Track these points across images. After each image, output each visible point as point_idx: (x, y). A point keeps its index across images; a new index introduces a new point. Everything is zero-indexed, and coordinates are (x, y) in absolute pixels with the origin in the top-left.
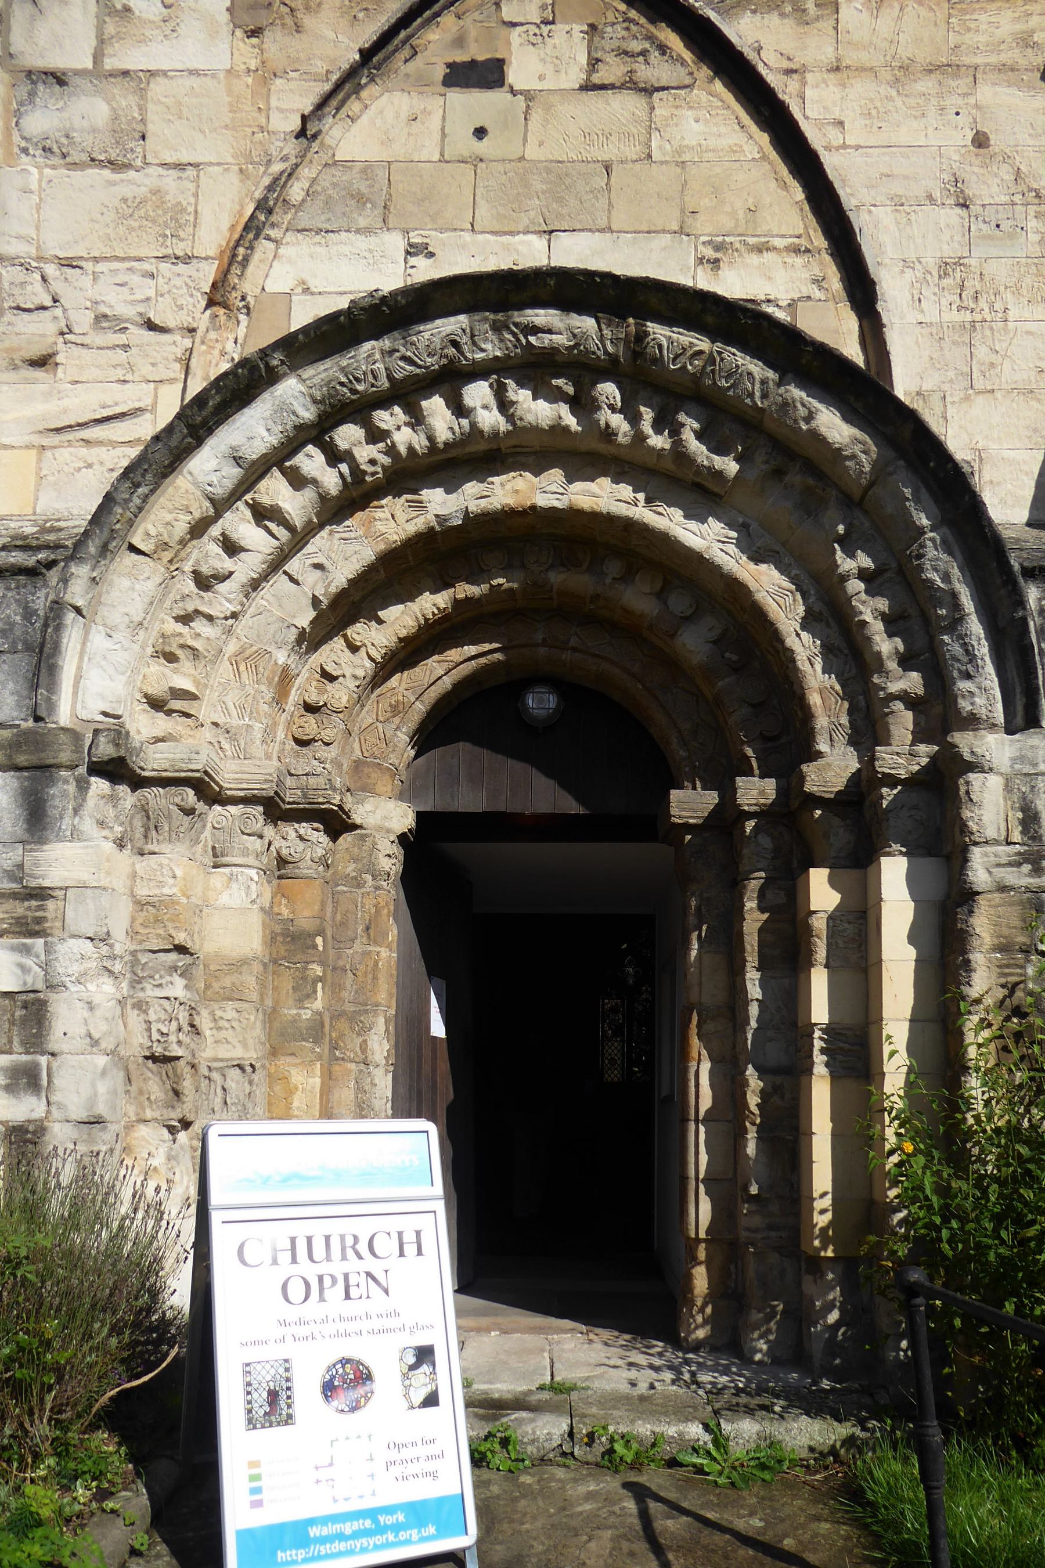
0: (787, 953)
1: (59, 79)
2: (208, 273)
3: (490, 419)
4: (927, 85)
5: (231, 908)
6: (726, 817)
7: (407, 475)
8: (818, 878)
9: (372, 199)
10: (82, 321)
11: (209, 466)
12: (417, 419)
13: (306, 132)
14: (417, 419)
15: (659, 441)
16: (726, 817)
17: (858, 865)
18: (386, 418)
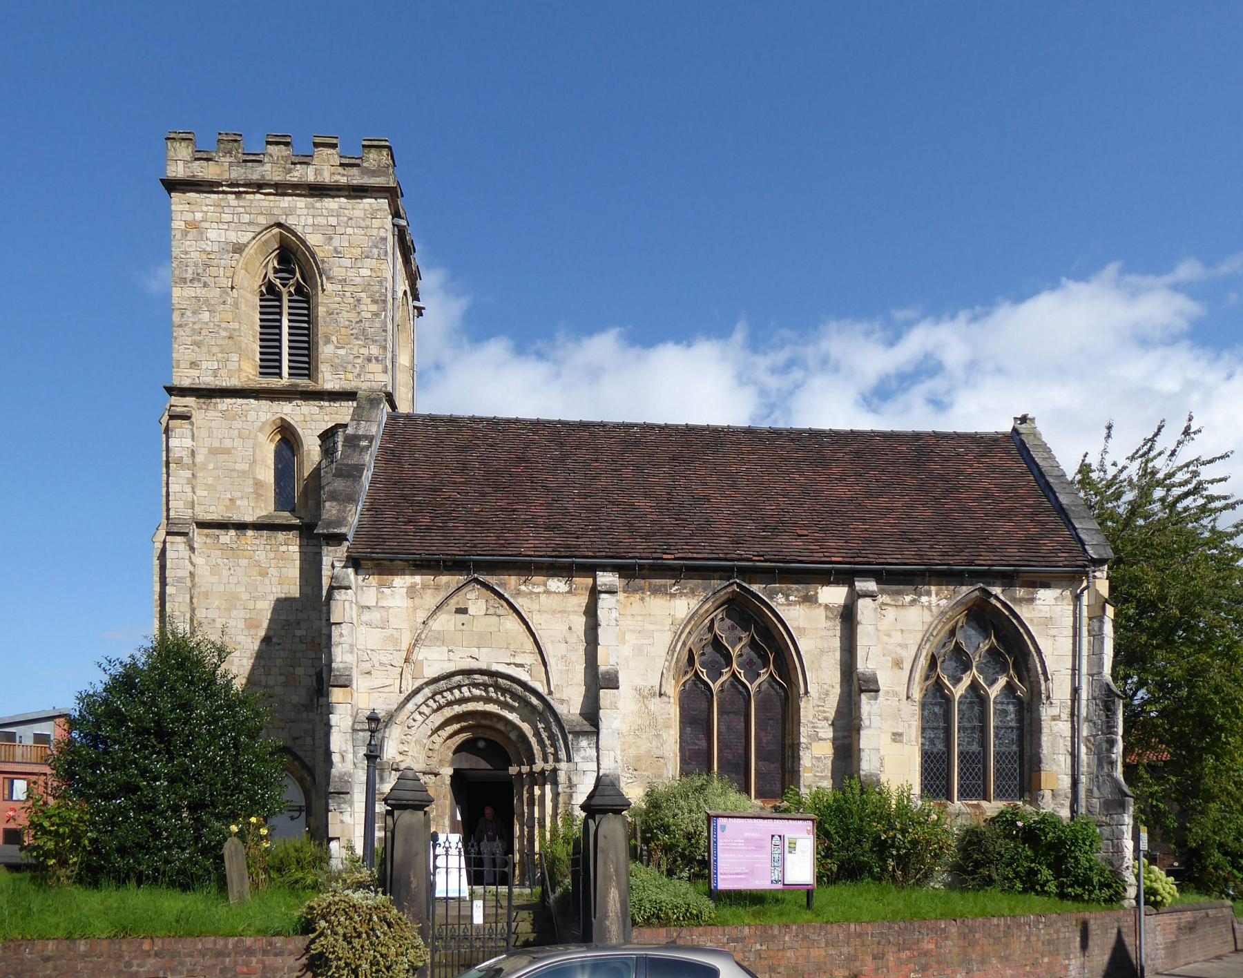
0: (531, 803)
3: (467, 694)
4: (559, 615)
6: (520, 774)
7: (450, 704)
8: (536, 788)
11: (410, 706)
15: (502, 699)
16: (520, 774)
17: (542, 786)
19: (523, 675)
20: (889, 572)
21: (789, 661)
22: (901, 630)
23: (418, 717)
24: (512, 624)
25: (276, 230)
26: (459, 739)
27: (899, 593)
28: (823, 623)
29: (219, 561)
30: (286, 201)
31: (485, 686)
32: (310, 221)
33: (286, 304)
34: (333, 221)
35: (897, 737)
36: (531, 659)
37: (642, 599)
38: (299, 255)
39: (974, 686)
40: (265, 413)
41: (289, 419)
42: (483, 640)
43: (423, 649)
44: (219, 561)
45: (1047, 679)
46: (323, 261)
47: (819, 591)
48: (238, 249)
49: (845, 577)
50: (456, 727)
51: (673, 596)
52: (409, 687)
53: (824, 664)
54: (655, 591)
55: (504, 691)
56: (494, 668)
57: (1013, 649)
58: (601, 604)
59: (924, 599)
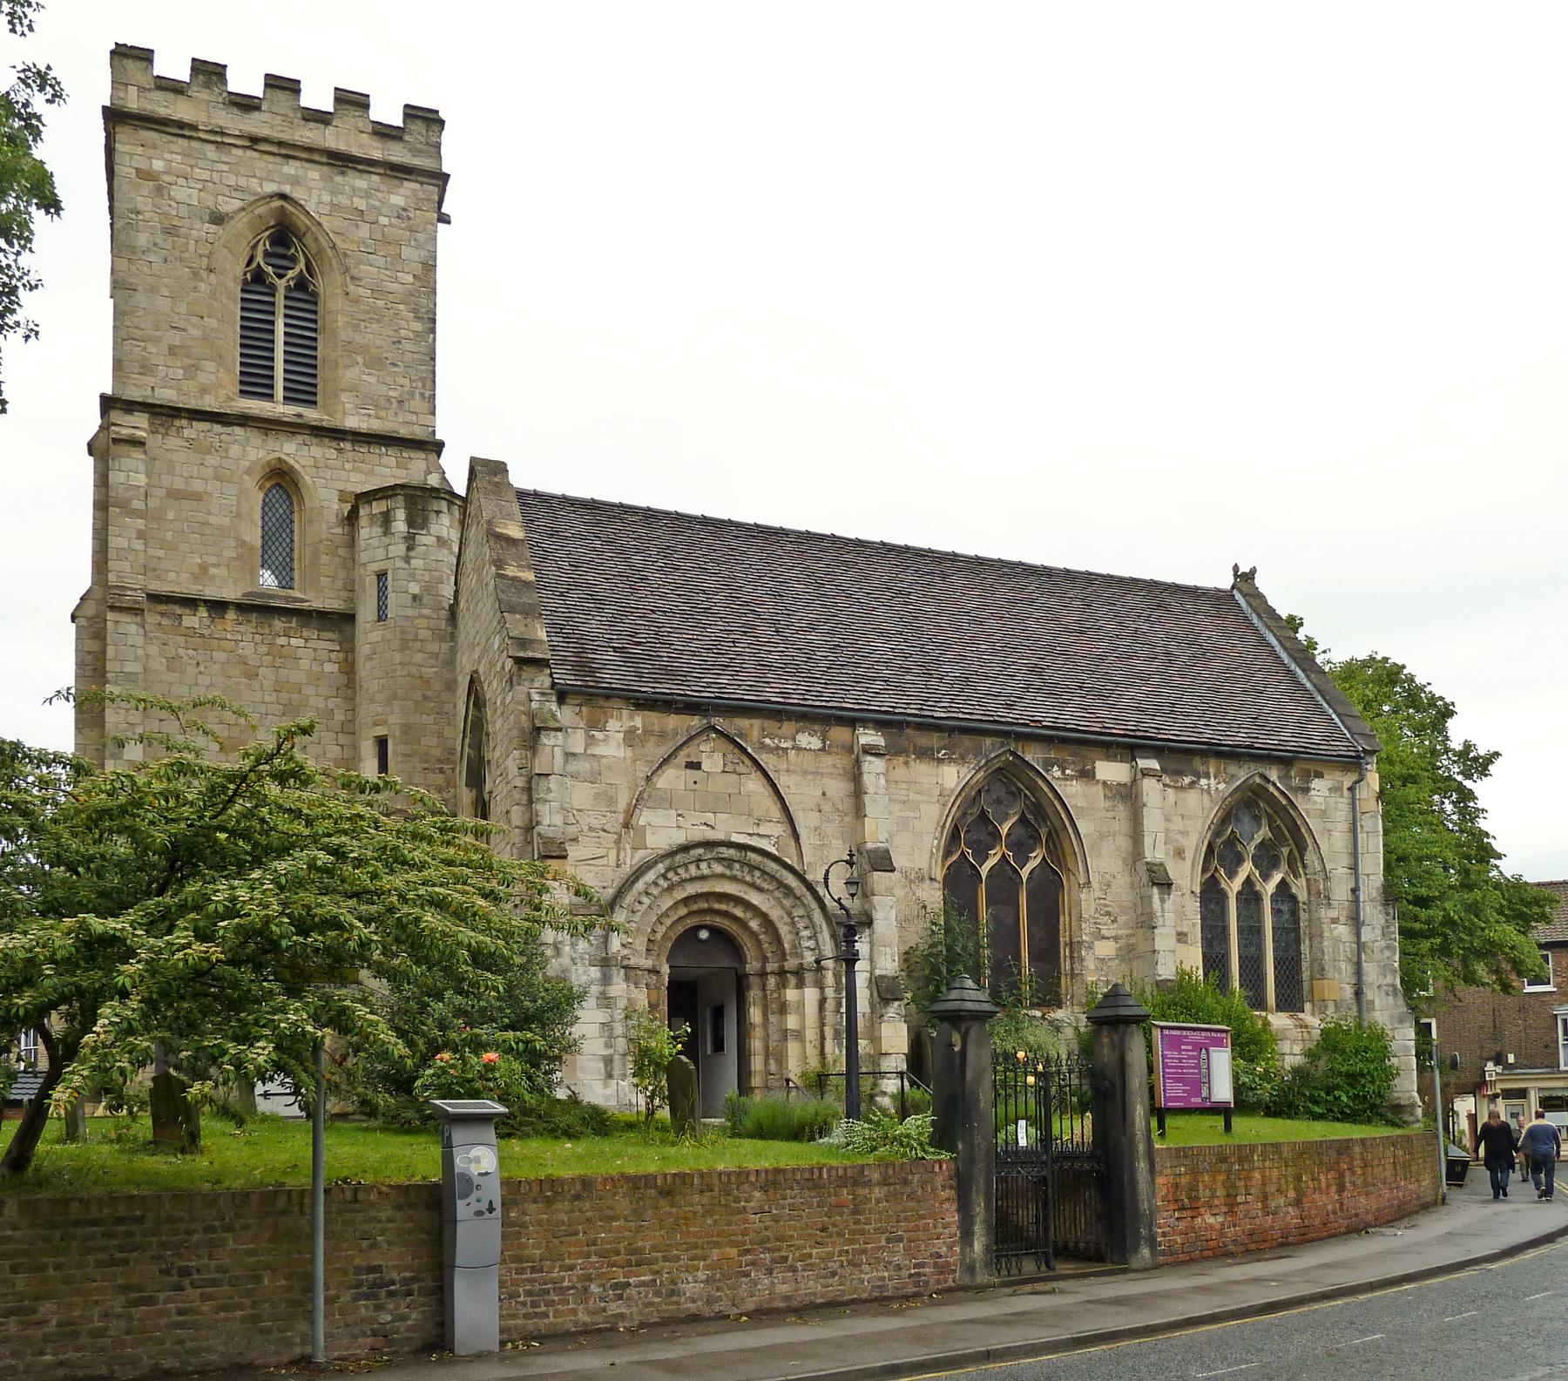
1: (574, 755)
2: (621, 818)
3: (706, 871)
5: (641, 998)
9: (668, 801)
10: (586, 828)
11: (640, 886)
12: (687, 870)
13: (648, 779)
14: (687, 870)
18: (680, 871)
19: (773, 850)
20: (1171, 750)
21: (1066, 845)
22: (1180, 816)
23: (645, 900)
24: (754, 785)
25: (278, 203)
26: (680, 929)
27: (1180, 773)
28: (1102, 803)
29: (182, 651)
30: (291, 168)
31: (728, 862)
32: (326, 198)
33: (280, 301)
34: (361, 204)
35: (1181, 937)
36: (777, 829)
37: (906, 763)
38: (308, 240)
39: (1248, 882)
40: (254, 451)
41: (292, 462)
42: (717, 804)
43: (646, 812)
44: (182, 651)
45: (1327, 878)
46: (345, 255)
47: (1098, 764)
48: (218, 219)
49: (1128, 748)
50: (683, 911)
51: (940, 761)
52: (632, 859)
53: (1104, 850)
54: (925, 754)
55: (753, 868)
56: (736, 838)
57: (1288, 841)
58: (865, 767)
59: (1203, 781)
